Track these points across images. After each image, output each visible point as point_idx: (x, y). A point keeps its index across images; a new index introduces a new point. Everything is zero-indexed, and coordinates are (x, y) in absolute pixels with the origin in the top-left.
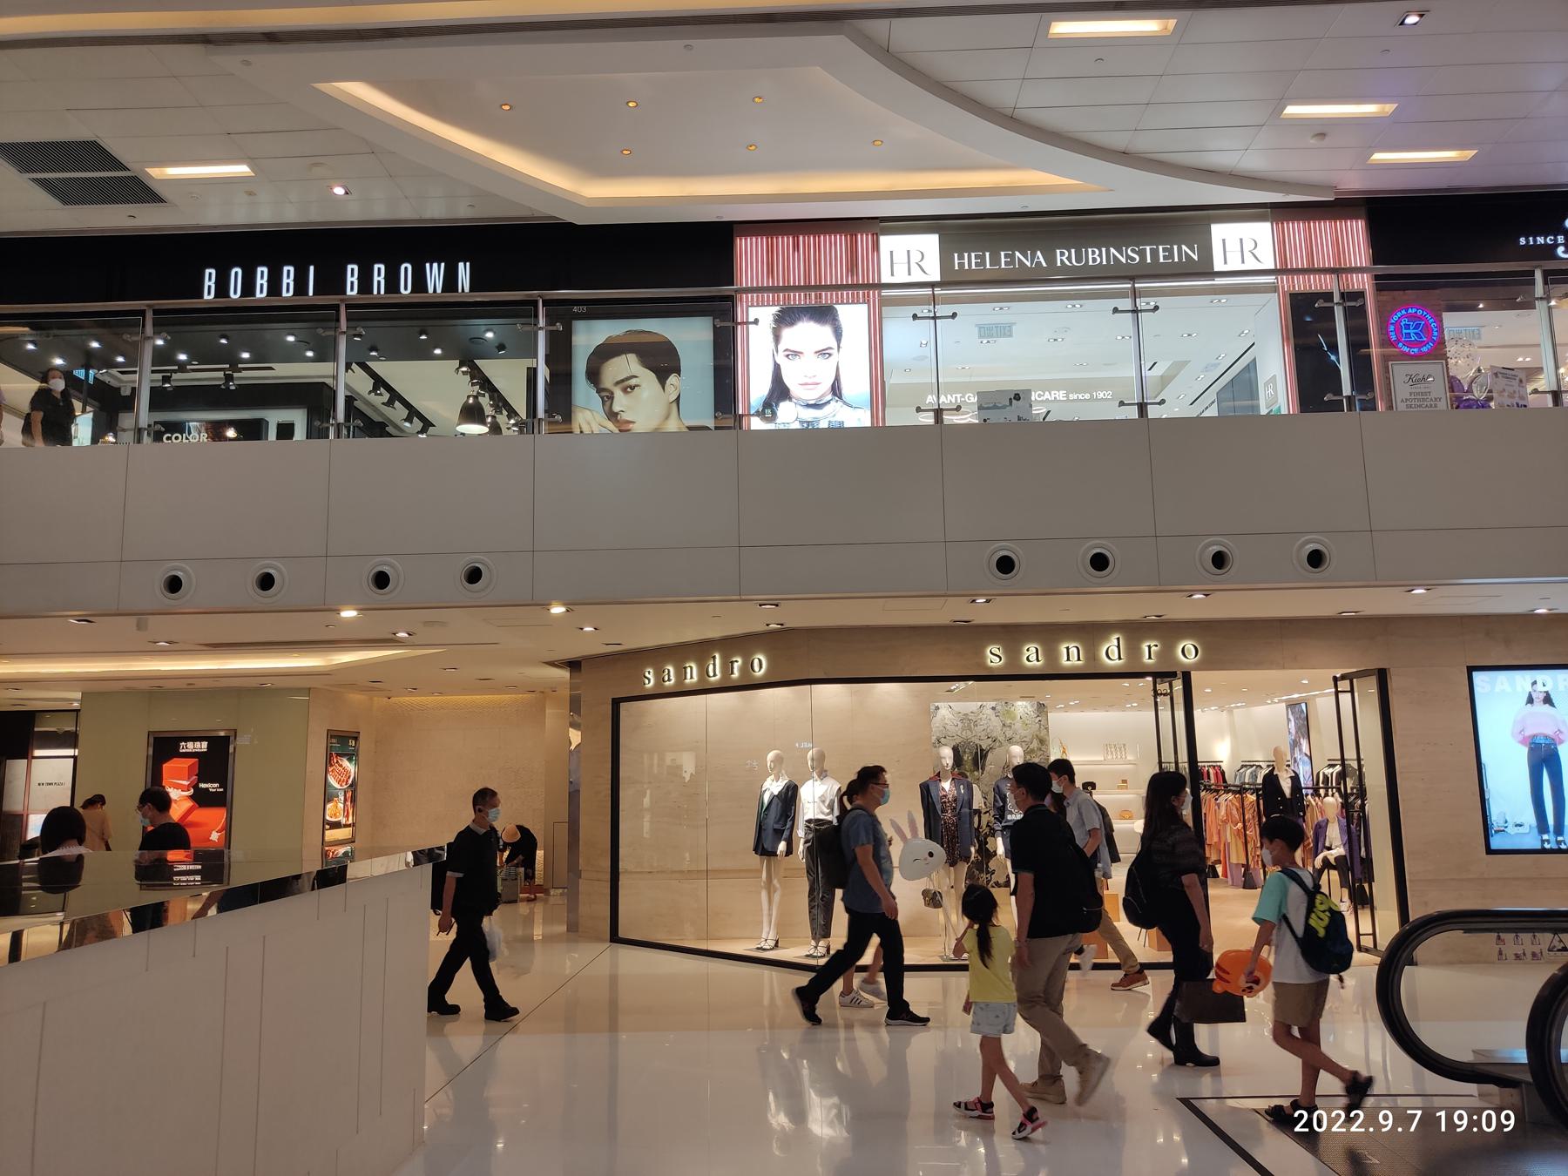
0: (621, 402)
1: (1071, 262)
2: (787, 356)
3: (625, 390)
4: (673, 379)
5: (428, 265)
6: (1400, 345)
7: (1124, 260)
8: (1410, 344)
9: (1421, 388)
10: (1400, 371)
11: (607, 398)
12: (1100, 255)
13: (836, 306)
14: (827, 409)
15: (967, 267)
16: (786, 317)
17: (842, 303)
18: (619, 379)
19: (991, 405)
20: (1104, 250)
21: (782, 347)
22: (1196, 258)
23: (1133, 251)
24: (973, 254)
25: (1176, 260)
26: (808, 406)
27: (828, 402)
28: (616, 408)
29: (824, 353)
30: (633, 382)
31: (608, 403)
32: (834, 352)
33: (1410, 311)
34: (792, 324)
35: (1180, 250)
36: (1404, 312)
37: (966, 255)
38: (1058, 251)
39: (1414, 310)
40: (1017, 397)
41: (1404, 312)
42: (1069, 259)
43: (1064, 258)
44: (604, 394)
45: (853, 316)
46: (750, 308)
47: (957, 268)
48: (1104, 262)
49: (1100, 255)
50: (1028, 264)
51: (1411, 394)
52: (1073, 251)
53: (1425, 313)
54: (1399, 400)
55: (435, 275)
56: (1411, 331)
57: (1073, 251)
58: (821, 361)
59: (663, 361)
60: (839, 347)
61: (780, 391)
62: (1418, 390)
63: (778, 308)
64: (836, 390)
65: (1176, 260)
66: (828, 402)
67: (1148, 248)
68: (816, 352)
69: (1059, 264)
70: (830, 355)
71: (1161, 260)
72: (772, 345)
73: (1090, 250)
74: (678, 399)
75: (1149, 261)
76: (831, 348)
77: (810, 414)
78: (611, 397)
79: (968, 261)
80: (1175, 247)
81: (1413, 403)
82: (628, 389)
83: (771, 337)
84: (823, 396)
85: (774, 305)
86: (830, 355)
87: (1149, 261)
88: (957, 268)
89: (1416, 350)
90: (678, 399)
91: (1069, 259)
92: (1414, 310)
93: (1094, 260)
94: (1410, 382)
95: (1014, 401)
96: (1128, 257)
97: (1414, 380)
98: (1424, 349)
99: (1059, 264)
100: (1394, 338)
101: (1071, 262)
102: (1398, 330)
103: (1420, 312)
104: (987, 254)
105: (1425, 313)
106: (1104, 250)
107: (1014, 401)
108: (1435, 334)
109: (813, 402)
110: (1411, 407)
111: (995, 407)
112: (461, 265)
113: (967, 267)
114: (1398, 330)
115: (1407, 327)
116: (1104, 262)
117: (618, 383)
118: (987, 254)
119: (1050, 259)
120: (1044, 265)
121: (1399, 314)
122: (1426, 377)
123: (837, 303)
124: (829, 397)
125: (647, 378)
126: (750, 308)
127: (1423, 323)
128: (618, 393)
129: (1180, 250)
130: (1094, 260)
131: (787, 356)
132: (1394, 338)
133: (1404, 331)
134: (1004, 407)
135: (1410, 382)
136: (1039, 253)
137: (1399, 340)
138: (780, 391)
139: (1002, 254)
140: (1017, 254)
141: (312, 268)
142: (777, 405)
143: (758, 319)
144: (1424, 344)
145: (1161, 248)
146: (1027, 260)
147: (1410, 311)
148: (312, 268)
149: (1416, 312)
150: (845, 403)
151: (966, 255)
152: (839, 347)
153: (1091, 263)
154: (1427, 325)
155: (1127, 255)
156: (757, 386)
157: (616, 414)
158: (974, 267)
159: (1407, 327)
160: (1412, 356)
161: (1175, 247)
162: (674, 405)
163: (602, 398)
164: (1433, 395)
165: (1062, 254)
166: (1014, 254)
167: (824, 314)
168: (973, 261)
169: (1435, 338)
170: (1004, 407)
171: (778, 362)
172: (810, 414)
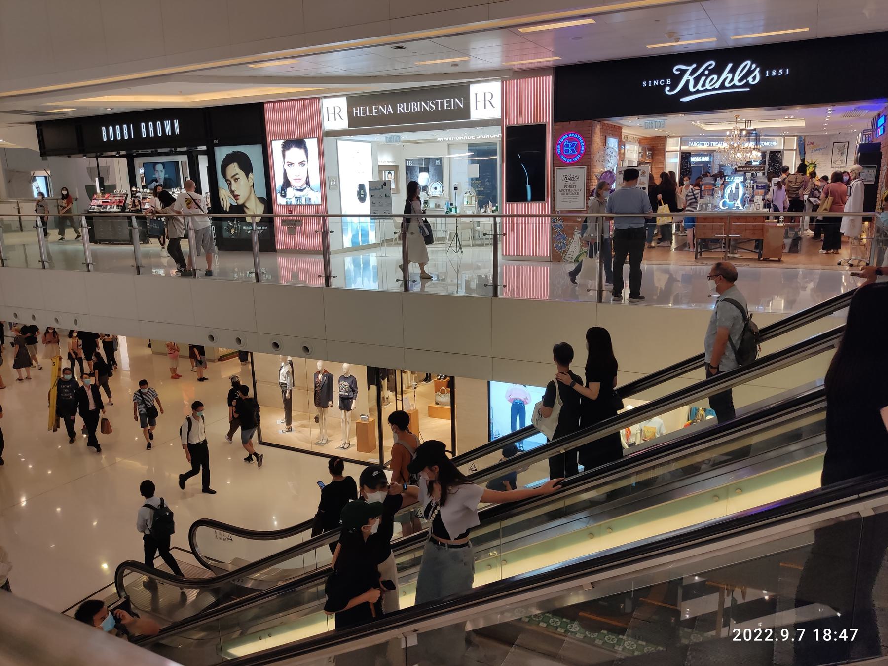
0: (234, 186)
1: (404, 111)
2: (288, 165)
3: (235, 180)
4: (250, 175)
5: (165, 122)
6: (562, 157)
7: (428, 109)
8: (567, 156)
9: (571, 183)
10: (561, 172)
11: (230, 184)
12: (417, 106)
13: (305, 139)
14: (305, 191)
15: (359, 115)
16: (287, 146)
17: (308, 138)
18: (233, 175)
19: (374, 188)
20: (419, 103)
21: (286, 161)
22: (462, 106)
23: (432, 103)
24: (361, 108)
25: (452, 108)
26: (298, 190)
27: (305, 188)
28: (233, 189)
29: (302, 164)
30: (237, 176)
31: (230, 186)
32: (306, 163)
33: (570, 135)
34: (289, 149)
35: (454, 101)
36: (566, 136)
37: (358, 108)
38: (398, 104)
39: (573, 135)
40: (385, 184)
41: (566, 136)
42: (403, 109)
43: (401, 109)
44: (228, 182)
45: (312, 144)
46: (273, 141)
47: (355, 116)
48: (419, 111)
49: (417, 106)
50: (385, 112)
51: (565, 186)
52: (405, 104)
53: (579, 136)
54: (558, 190)
55: (167, 124)
56: (569, 148)
57: (405, 104)
58: (300, 167)
59: (246, 167)
60: (307, 161)
61: (287, 184)
62: (569, 185)
63: (283, 141)
64: (307, 182)
65: (452, 108)
66: (305, 188)
67: (439, 101)
68: (299, 163)
69: (399, 112)
70: (304, 165)
71: (445, 108)
72: (282, 159)
73: (412, 103)
74: (253, 185)
75: (439, 109)
76: (304, 161)
77: (298, 194)
78: (231, 184)
79: (359, 111)
80: (452, 100)
81: (566, 192)
82: (236, 180)
83: (281, 155)
84: (303, 185)
85: (282, 139)
86: (304, 165)
87: (439, 109)
88: (355, 116)
89: (570, 160)
90: (253, 185)
91: (403, 109)
92: (573, 135)
93: (414, 109)
94: (566, 180)
95: (384, 186)
96: (430, 107)
97: (568, 178)
98: (576, 159)
99: (399, 112)
100: (559, 153)
101: (404, 111)
102: (562, 148)
103: (576, 136)
104: (367, 107)
105: (579, 136)
106: (419, 103)
107: (384, 186)
108: (583, 149)
109: (299, 188)
110: (564, 195)
111: (376, 189)
112: (175, 121)
113: (359, 115)
114: (562, 148)
115: (567, 145)
116: (419, 111)
117: (232, 177)
118: (367, 107)
119: (395, 109)
120: (392, 113)
121: (564, 137)
122: (574, 177)
123: (304, 138)
124: (305, 186)
125: (241, 174)
126: (273, 141)
127: (577, 142)
128: (233, 182)
129: (454, 101)
130: (414, 110)
131: (288, 165)
132: (559, 153)
133: (566, 148)
134: (379, 189)
135: (566, 180)
136: (390, 106)
137: (561, 154)
138: (287, 184)
139: (374, 107)
140: (380, 107)
141: (131, 125)
142: (286, 189)
143: (276, 146)
144: (575, 156)
145: (445, 100)
146: (384, 109)
147: (570, 135)
148: (131, 125)
149: (573, 136)
150: (311, 189)
151: (358, 108)
152: (307, 161)
153: (413, 111)
154: (579, 143)
155: (429, 105)
156: (279, 182)
157: (233, 192)
158: (362, 115)
159: (567, 145)
160: (567, 163)
161: (452, 100)
162: (252, 187)
163: (228, 184)
164: (577, 188)
165: (400, 106)
166: (379, 107)
167: (300, 143)
168: (362, 112)
169: (582, 152)
170: (379, 189)
171: (285, 168)
172: (298, 194)
